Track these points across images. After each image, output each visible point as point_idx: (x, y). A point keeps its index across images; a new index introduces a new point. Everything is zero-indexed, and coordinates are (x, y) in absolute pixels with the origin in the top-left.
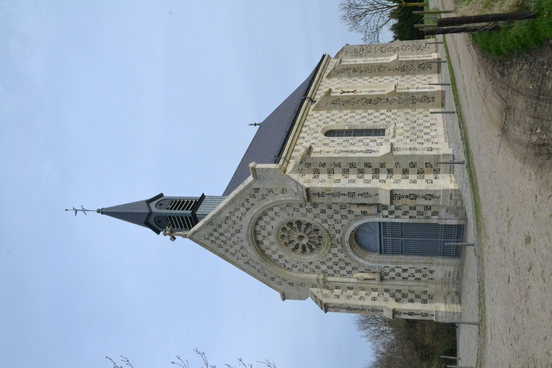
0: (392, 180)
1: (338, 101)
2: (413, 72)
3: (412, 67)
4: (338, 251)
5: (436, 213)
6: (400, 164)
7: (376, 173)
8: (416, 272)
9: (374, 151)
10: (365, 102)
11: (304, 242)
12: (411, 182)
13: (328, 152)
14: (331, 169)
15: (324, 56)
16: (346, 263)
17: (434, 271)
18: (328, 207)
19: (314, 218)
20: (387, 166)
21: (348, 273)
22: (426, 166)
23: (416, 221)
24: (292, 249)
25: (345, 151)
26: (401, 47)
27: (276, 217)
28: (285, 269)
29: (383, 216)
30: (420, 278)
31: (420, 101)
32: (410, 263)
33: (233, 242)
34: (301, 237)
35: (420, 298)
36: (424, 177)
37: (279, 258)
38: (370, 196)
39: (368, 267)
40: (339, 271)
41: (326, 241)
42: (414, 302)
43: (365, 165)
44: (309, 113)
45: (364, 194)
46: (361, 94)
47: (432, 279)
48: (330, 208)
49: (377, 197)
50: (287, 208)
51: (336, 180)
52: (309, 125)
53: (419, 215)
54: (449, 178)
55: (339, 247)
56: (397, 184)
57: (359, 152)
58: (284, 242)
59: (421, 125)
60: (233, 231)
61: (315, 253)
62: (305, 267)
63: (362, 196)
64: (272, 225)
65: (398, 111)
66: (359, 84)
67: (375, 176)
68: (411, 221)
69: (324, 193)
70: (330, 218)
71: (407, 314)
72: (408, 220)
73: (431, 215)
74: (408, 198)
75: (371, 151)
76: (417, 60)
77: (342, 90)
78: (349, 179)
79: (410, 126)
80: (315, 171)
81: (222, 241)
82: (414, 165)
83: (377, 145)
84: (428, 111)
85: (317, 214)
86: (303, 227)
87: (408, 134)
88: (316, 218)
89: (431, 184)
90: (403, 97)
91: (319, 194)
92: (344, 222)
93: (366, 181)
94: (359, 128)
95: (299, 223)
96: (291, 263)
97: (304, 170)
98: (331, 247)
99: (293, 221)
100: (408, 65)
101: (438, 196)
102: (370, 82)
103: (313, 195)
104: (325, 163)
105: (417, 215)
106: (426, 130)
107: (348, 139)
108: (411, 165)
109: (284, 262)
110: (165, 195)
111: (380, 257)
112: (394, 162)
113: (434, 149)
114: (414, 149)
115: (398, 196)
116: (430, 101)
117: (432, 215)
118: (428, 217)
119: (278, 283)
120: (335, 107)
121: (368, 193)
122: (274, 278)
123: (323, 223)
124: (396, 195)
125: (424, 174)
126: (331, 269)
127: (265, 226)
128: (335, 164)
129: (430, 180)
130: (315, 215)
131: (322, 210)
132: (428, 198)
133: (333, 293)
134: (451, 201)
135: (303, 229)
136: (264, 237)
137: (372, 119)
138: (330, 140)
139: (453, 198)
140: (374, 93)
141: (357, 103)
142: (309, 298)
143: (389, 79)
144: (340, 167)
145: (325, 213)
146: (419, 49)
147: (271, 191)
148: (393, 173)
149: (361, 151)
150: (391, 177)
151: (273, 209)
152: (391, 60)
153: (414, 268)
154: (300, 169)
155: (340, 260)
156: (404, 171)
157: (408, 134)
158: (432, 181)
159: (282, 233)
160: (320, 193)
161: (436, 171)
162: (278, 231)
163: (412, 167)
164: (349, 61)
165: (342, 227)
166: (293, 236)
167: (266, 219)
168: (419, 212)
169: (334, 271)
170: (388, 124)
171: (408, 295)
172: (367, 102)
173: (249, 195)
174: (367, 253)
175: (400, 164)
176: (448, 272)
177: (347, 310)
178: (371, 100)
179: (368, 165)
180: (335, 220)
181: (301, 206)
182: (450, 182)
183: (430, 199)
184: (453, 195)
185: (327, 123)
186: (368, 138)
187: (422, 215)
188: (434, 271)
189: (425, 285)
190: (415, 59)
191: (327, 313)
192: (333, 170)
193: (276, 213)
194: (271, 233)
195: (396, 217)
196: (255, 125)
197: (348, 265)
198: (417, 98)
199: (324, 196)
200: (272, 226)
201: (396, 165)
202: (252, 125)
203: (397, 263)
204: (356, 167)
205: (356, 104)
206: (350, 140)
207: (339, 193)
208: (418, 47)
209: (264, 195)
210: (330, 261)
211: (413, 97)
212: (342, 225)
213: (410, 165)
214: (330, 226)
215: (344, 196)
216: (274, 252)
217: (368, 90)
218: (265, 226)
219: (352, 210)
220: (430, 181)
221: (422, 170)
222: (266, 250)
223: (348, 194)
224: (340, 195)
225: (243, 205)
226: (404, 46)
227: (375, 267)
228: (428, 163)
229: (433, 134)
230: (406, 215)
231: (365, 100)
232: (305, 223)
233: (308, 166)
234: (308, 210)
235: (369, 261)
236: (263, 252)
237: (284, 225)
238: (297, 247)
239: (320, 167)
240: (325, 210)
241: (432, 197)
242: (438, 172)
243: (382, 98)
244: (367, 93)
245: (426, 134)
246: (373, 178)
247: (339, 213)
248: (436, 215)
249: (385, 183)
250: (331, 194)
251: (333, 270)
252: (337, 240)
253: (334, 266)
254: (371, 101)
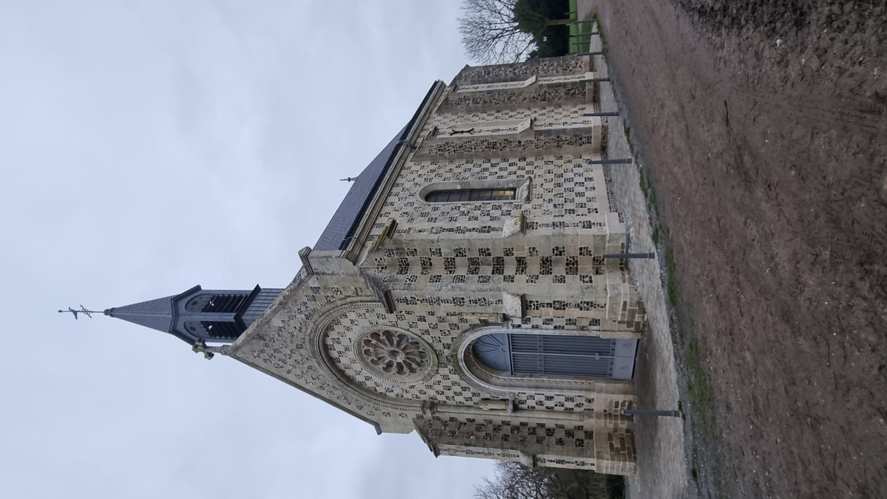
0: (524, 277)
1: (447, 146)
2: (558, 101)
3: (557, 94)
4: (450, 372)
5: (596, 322)
6: (537, 249)
7: (498, 264)
8: (566, 401)
9: (494, 229)
10: (486, 148)
11: (400, 359)
12: (556, 279)
13: (420, 231)
14: (426, 258)
15: (436, 83)
16: (462, 387)
17: (593, 399)
20: (517, 254)
21: (467, 400)
22: (581, 254)
23: (563, 333)
25: (447, 230)
26: (541, 68)
27: (354, 327)
29: (513, 326)
30: (573, 409)
31: (568, 144)
32: (557, 388)
33: (296, 361)
34: (394, 353)
35: (573, 437)
36: (577, 270)
38: (489, 304)
39: (495, 393)
40: (453, 397)
42: (564, 444)
43: (479, 251)
44: (406, 166)
45: (479, 300)
46: (482, 134)
47: (590, 410)
48: (432, 315)
49: (500, 305)
51: (435, 276)
52: (403, 184)
53: (570, 324)
54: (621, 275)
55: (450, 367)
56: (533, 283)
57: (470, 231)
59: (570, 180)
60: (293, 346)
62: (405, 392)
63: (476, 303)
65: (536, 160)
66: (481, 121)
67: (497, 269)
68: (557, 333)
69: (415, 299)
70: (433, 328)
71: (554, 461)
72: (552, 331)
73: (588, 325)
74: (551, 307)
75: (489, 229)
76: (563, 83)
77: (453, 130)
78: (454, 275)
79: (553, 182)
80: (402, 261)
81: (280, 360)
82: (561, 252)
83: (502, 215)
84: (581, 158)
85: (414, 323)
86: (395, 340)
87: (551, 196)
89: (589, 284)
90: (542, 137)
91: (407, 301)
92: (455, 333)
93: (481, 279)
94: (478, 188)
95: (388, 334)
97: (383, 260)
99: (380, 331)
100: (551, 91)
101: (603, 305)
102: (497, 118)
103: (398, 302)
104: (415, 250)
105: (567, 324)
106: (581, 189)
107: (459, 205)
108: (555, 252)
109: (375, 386)
110: (203, 288)
111: (512, 378)
112: (527, 248)
113: (594, 224)
114: (560, 224)
115: (534, 305)
116: (583, 143)
117: (590, 325)
118: (584, 327)
119: (369, 413)
120: (443, 155)
121: (484, 299)
122: (363, 407)
123: (424, 334)
124: (531, 302)
125: (577, 265)
127: (339, 338)
128: (434, 250)
129: (587, 276)
130: (410, 323)
131: (420, 316)
132: (585, 307)
133: (447, 428)
134: (624, 312)
135: (395, 343)
136: (340, 353)
137: (496, 173)
138: (431, 207)
139: (628, 307)
140: (500, 133)
141: (475, 149)
142: (415, 431)
143: (523, 112)
144: (441, 256)
145: (425, 321)
146: (566, 70)
147: (338, 291)
148: (526, 264)
149: (474, 229)
150: (522, 271)
151: (346, 316)
152: (525, 85)
153: (563, 395)
154: (379, 259)
155: (454, 383)
156: (543, 261)
157: (551, 196)
158: (591, 277)
159: (366, 348)
160: (409, 299)
161: (597, 260)
162: (359, 345)
163: (556, 255)
164: (467, 89)
165: (452, 341)
166: (382, 351)
167: (338, 328)
168: (570, 320)
170: (521, 180)
171: (556, 431)
172: (489, 147)
173: (306, 296)
174: (493, 373)
175: (537, 249)
176: (614, 402)
177: (467, 453)
178: (495, 144)
179: (485, 252)
180: (441, 331)
182: (621, 281)
183: (588, 309)
184: (628, 303)
185: (430, 180)
186: (489, 204)
187: (575, 324)
188: (593, 399)
189: (579, 419)
190: (561, 81)
191: (438, 457)
192: (430, 259)
193: (352, 322)
195: (533, 327)
196: (349, 180)
197: (465, 390)
198: (564, 139)
199: (416, 304)
201: (530, 252)
202: (345, 180)
203: (537, 387)
204: (465, 256)
205: (473, 150)
206: (462, 206)
207: (439, 299)
208: (565, 66)
209: (328, 296)
211: (558, 137)
212: (452, 338)
213: (554, 252)
215: (446, 304)
216: (358, 373)
217: (491, 128)
218: (339, 338)
219: (465, 317)
220: (587, 279)
221: (574, 259)
222: (345, 370)
223: (454, 300)
224: (441, 302)
225: (299, 311)
226: (545, 65)
227: (505, 393)
228: (585, 248)
229: (589, 194)
230: (548, 324)
231: (486, 143)
232: (398, 334)
233: (390, 254)
235: (495, 385)
236: (342, 372)
238: (390, 365)
239: (408, 255)
240: (425, 317)
241: (592, 306)
242: (600, 262)
243: (512, 140)
244: (489, 133)
245: (579, 194)
246: (493, 273)
247: (446, 322)
248: (596, 325)
249: (513, 281)
250: (426, 300)
252: (447, 358)
254: (496, 145)
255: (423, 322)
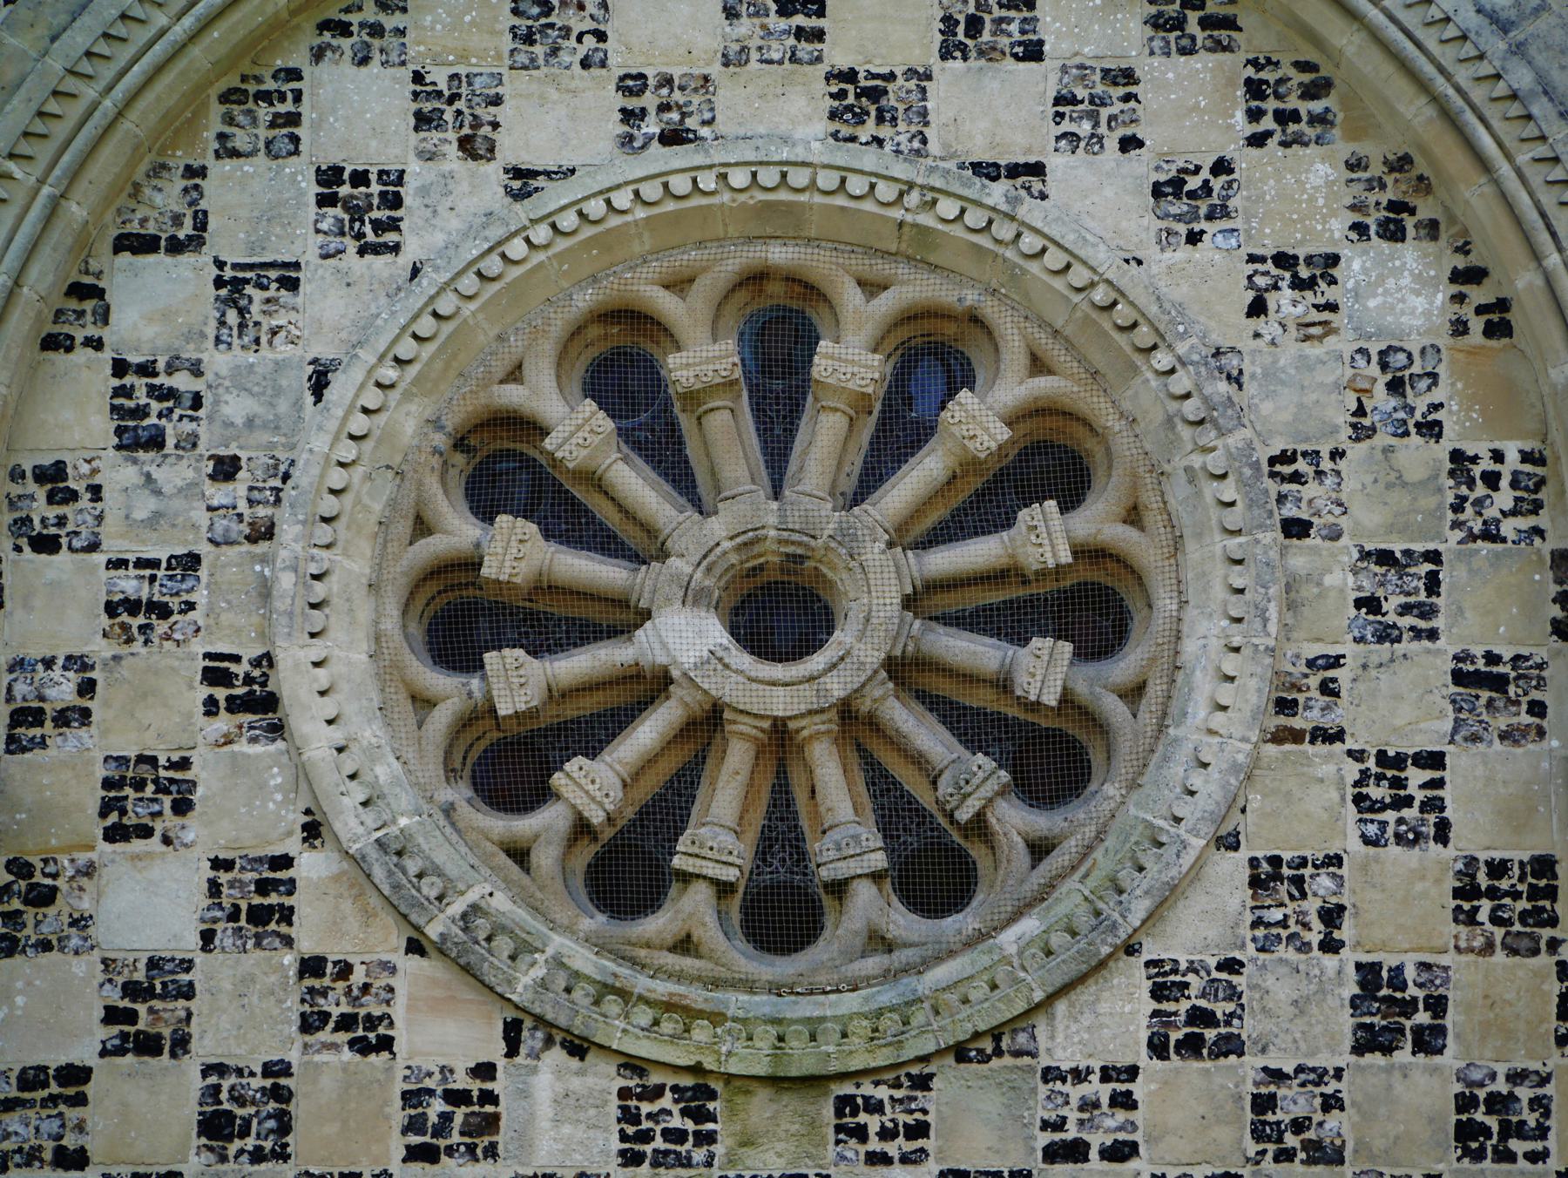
18: (1497, 1103)
19: (1256, 847)
24: (530, 428)
28: (83, 245)
37: (330, 176)
41: (735, 1002)
48: (1467, 1133)
50: (1433, 455)
58: (666, 304)
61: (447, 794)
62: (130, 584)
64: (1057, 164)
70: (1263, 1103)
85: (1332, 915)
88: (1255, 883)
96: (218, 361)
98: (633, 1065)
123: (1158, 993)
126: (112, 1015)
127: (1033, 52)
131: (1437, 1005)
145: (1369, 1041)
151: (1392, 232)
169: (76, 1075)
181: (1499, 683)
194: (901, 135)
200: (1037, 170)
210: (308, 1025)
214: (1104, 1092)
218: (1033, 52)
232: (1114, 709)
234: (1416, 777)
237: (1038, 365)
240: (1428, 1042)
251: (84, 1052)
253: (197, 1083)
255: (1346, 1022)
